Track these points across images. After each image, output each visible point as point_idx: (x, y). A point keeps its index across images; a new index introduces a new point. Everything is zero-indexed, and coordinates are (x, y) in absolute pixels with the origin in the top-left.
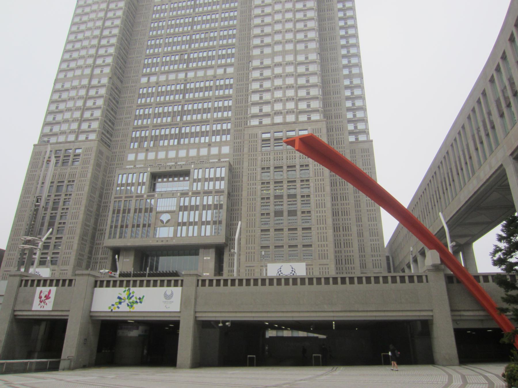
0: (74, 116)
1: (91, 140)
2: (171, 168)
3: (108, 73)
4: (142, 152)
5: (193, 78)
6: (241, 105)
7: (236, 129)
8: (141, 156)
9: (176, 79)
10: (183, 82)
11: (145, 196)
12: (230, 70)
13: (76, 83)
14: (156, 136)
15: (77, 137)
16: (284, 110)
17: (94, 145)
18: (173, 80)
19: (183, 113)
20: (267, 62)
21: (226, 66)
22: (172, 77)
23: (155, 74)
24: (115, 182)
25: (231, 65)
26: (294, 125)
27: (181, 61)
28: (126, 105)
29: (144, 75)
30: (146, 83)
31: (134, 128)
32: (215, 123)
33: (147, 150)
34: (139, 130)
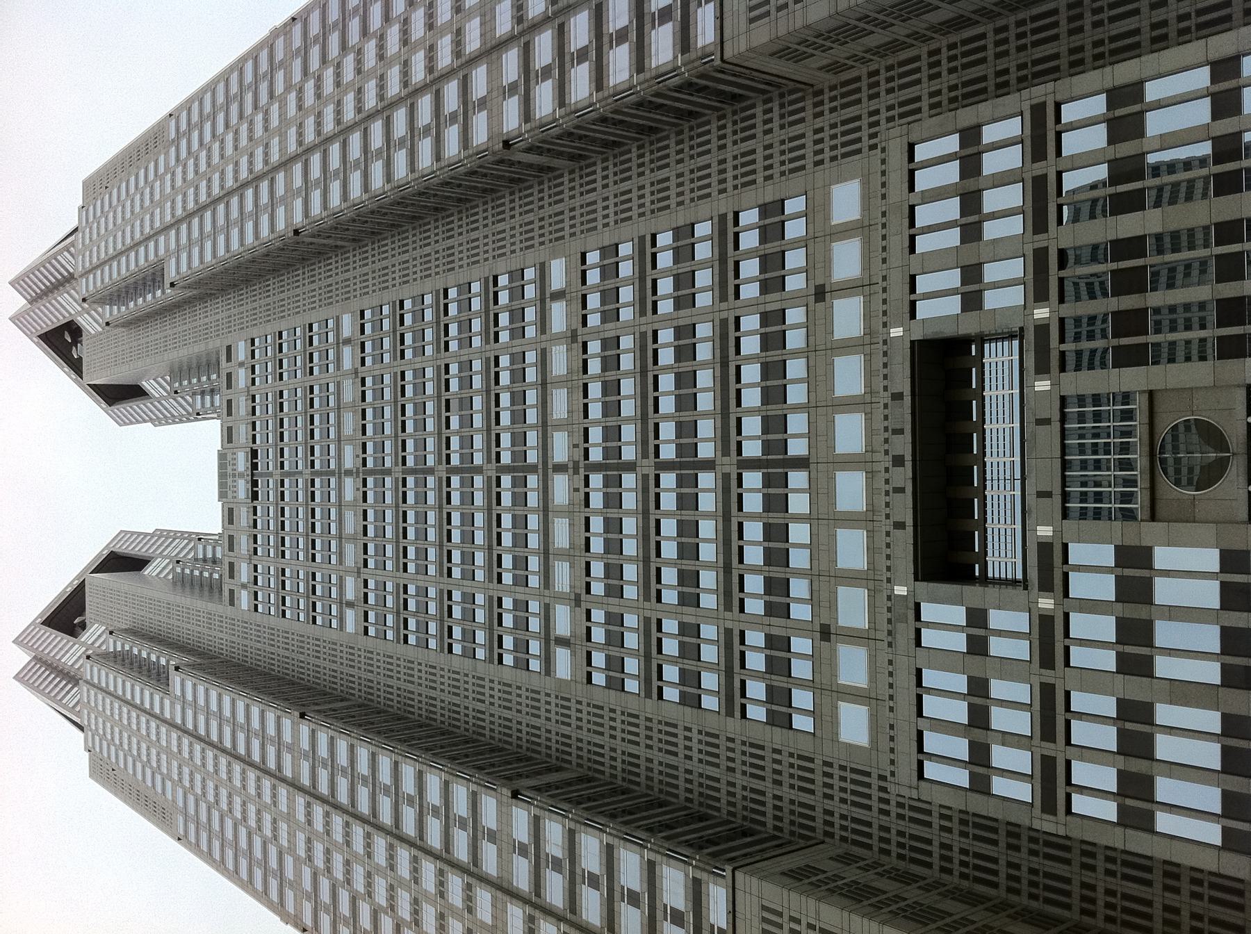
2: (898, 461)
3: (500, 803)
11: (1046, 603)
12: (558, 276)
24: (956, 803)
30: (573, 654)
31: (730, 713)
33: (825, 633)
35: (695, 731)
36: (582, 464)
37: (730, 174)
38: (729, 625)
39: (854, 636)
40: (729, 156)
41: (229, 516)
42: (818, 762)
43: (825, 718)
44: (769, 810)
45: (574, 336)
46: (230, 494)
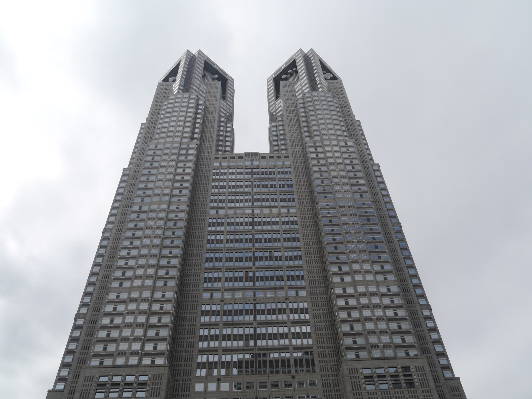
0: (136, 334)
1: (159, 366)
3: (173, 287)
4: (212, 382)
5: (263, 298)
6: (321, 332)
7: (320, 359)
8: (212, 387)
9: (244, 298)
10: (251, 301)
12: (303, 293)
13: (135, 295)
14: (228, 363)
15: (140, 360)
16: (380, 343)
17: (165, 372)
18: (241, 298)
19: (256, 337)
20: (350, 290)
21: (297, 288)
22: (239, 295)
23: (218, 290)
25: (303, 288)
26: (394, 360)
27: (247, 279)
28: (187, 323)
29: (206, 290)
30: (209, 299)
32: (296, 351)
34: (206, 353)
35: (194, 340)
36: (256, 302)
37: (322, 350)
38: (219, 351)
39: (218, 387)
40: (325, 350)
41: (240, 157)
42: (191, 377)
43: (200, 379)
44: (178, 363)
45: (287, 299)
46: (246, 158)
